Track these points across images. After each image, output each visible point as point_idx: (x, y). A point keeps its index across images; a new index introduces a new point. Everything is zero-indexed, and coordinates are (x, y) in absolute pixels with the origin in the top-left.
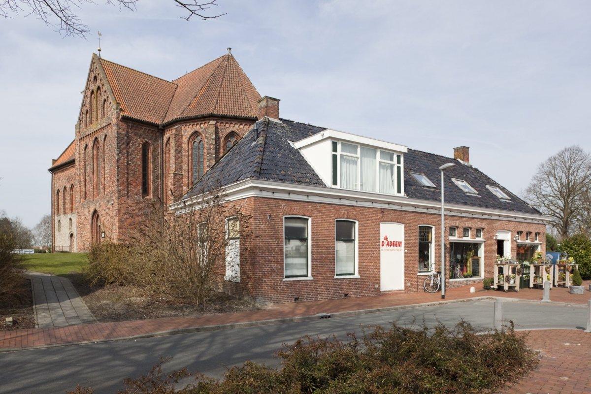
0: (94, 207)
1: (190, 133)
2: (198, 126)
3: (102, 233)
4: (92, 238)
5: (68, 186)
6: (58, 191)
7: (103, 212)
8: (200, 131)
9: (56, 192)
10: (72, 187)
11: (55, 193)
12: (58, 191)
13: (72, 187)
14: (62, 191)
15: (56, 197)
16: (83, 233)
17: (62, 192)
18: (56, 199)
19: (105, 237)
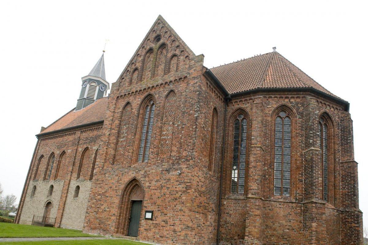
0: (133, 175)
1: (275, 106)
2: (287, 100)
3: (147, 212)
4: (120, 216)
5: (57, 152)
6: (42, 156)
7: (154, 183)
8: (290, 105)
9: (38, 157)
10: (64, 153)
11: (37, 159)
12: (42, 156)
13: (64, 153)
14: (46, 157)
15: (37, 162)
16: (102, 207)
17: (47, 158)
18: (36, 164)
19: (151, 219)
